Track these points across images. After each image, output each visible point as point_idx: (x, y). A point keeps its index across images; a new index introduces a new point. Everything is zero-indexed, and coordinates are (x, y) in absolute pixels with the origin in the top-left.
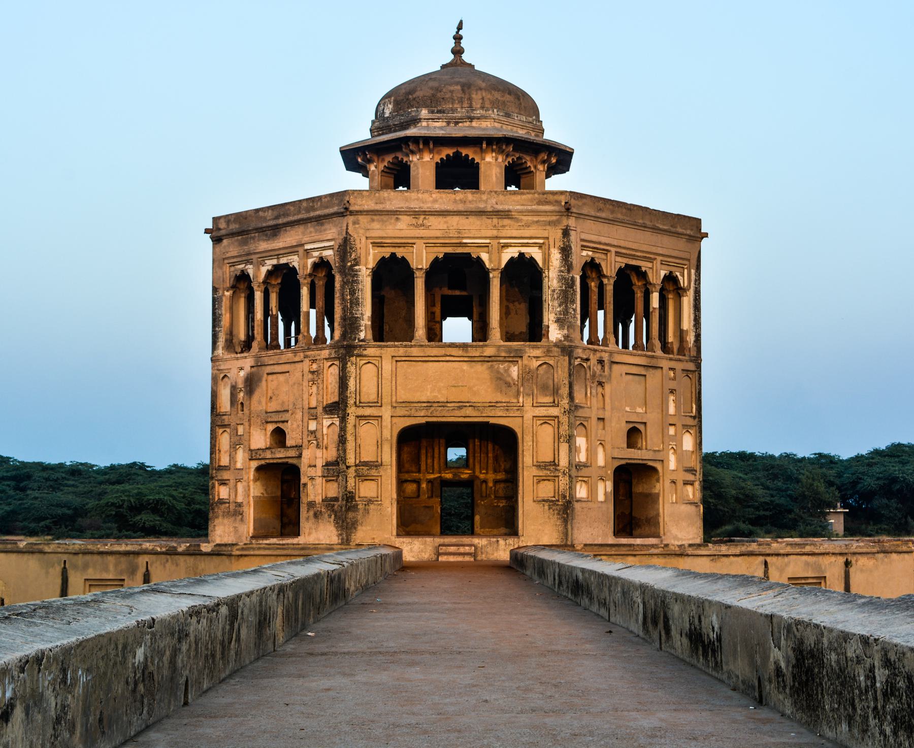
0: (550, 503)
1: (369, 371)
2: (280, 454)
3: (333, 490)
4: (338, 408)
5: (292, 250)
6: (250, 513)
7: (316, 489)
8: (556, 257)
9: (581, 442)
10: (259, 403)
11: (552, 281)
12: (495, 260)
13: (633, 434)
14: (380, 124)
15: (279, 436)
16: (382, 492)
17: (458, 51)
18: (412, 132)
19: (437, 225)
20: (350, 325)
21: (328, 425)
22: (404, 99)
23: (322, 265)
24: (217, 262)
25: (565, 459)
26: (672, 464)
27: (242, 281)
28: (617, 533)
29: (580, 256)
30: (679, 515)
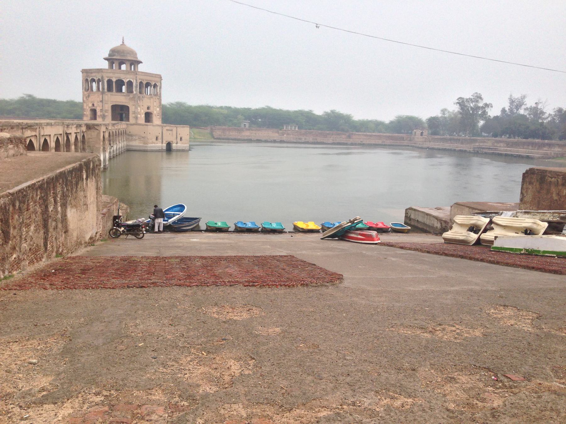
0: (134, 117)
1: (106, 97)
2: (93, 108)
3: (101, 114)
4: (102, 101)
5: (95, 76)
6: (89, 116)
7: (99, 113)
8: (135, 81)
9: (139, 108)
10: (90, 99)
11: (134, 84)
12: (126, 81)
13: (148, 108)
14: (110, 55)
15: (93, 105)
16: (109, 114)
17: (123, 42)
18: (114, 57)
19: (117, 75)
20: (103, 89)
21: (100, 104)
22: (113, 52)
23: (99, 79)
24: (83, 76)
25: (137, 112)
26: (155, 112)
27: (87, 80)
28: (146, 122)
29: (139, 81)
30: (157, 120)
